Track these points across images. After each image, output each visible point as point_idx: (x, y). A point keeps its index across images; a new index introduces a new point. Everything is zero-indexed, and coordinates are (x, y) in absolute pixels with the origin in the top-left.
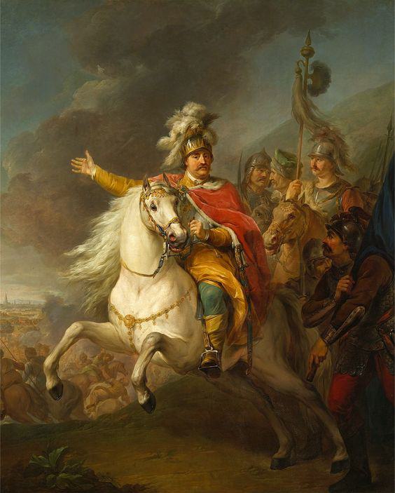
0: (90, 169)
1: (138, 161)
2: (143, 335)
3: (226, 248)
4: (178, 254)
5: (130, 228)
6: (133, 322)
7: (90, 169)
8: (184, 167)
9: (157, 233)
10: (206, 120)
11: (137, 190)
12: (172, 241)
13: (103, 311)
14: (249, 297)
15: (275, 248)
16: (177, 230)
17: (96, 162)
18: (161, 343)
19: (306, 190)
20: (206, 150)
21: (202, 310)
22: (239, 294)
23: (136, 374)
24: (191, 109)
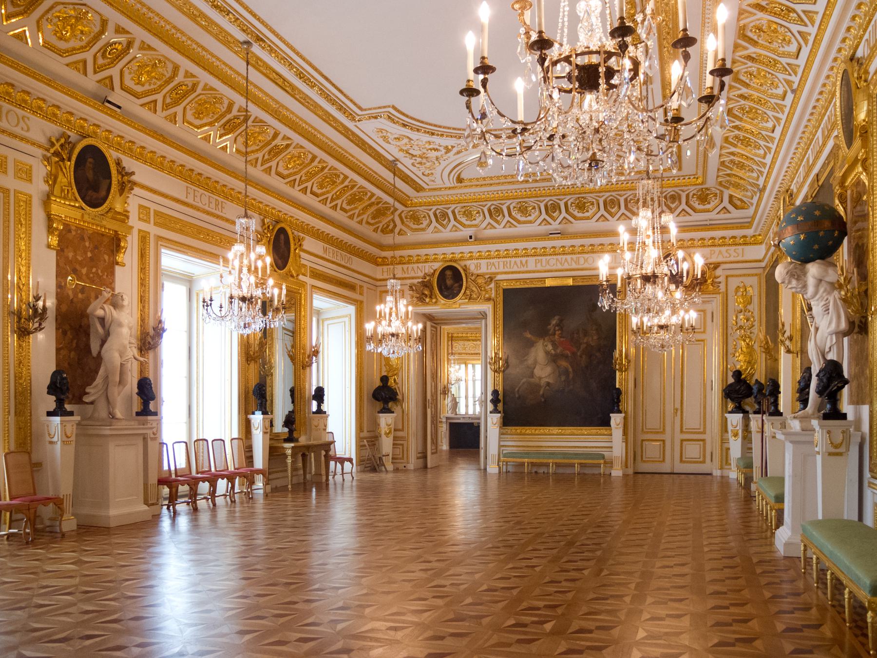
1: (543, 333)
2: (543, 382)
3: (567, 357)
4: (553, 359)
5: (540, 352)
6: (540, 378)
8: (555, 334)
9: (547, 353)
10: (561, 321)
11: (541, 342)
12: (551, 355)
14: (573, 370)
15: (581, 357)
16: (553, 352)
18: (548, 384)
19: (590, 339)
20: (561, 329)
21: (560, 376)
22: (571, 370)
23: (541, 393)
24: (557, 318)
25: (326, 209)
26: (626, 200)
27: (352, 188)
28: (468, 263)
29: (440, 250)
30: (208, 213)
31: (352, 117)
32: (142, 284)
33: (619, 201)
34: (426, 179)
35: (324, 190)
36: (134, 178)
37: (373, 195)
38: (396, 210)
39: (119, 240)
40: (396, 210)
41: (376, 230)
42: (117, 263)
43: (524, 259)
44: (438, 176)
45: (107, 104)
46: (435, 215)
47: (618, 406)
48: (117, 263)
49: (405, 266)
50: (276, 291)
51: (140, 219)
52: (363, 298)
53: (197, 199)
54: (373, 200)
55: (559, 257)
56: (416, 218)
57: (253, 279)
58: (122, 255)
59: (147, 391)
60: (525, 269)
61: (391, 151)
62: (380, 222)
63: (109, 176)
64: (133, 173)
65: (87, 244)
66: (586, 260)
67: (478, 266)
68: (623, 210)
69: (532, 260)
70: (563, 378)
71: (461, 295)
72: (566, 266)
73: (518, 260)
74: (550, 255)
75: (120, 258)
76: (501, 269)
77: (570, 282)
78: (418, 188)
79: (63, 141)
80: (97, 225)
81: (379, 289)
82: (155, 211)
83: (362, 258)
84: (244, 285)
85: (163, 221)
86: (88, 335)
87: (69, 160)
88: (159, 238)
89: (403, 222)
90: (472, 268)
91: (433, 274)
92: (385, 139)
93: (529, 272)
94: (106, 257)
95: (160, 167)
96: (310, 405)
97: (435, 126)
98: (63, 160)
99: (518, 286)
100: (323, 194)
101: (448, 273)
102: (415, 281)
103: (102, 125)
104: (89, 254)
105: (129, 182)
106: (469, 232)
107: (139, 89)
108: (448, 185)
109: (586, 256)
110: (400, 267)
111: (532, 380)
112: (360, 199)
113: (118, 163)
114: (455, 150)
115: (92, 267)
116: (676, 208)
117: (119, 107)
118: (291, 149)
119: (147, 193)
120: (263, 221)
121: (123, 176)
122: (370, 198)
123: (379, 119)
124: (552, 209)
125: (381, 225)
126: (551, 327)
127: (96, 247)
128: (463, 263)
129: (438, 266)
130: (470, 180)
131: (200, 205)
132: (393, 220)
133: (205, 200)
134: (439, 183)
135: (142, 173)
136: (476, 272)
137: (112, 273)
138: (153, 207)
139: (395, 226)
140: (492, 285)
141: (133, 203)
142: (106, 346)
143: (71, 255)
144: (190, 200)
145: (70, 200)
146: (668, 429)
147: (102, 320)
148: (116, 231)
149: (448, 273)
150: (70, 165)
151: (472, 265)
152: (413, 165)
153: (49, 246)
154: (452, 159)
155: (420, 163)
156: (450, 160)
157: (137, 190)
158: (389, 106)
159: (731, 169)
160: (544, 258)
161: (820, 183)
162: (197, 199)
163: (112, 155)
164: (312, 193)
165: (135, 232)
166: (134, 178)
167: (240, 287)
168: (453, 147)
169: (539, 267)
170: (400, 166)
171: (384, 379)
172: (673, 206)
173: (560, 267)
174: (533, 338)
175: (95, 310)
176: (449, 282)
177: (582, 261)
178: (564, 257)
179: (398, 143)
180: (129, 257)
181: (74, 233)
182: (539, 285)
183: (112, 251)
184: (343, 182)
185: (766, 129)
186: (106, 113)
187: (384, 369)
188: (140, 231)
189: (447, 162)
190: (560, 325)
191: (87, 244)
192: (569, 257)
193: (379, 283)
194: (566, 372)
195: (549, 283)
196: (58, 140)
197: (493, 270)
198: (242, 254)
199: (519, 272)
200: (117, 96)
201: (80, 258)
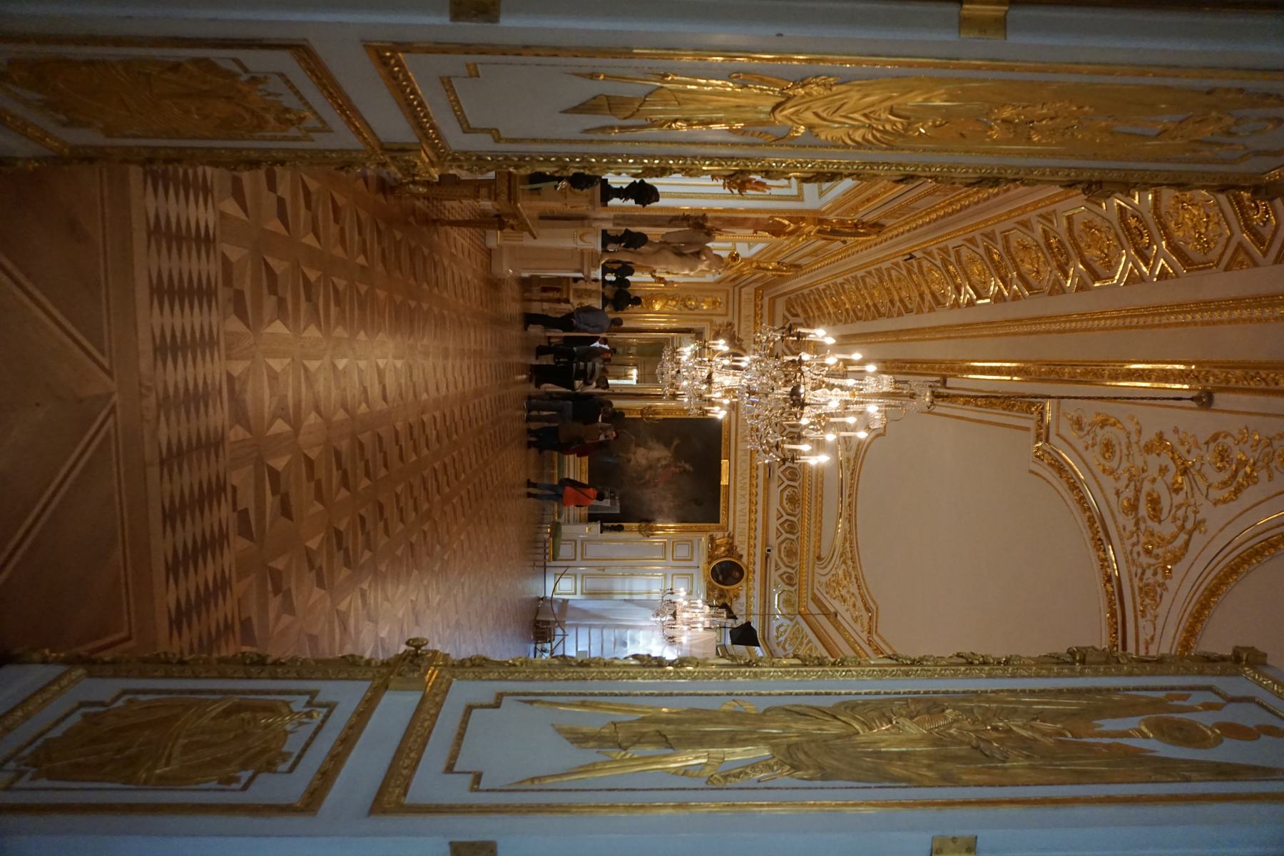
0: (676, 442)
2: (632, 456)
7: (676, 442)
9: (659, 460)
13: (638, 445)
18: (629, 461)
33: (793, 534)
66: (743, 496)
68: (785, 535)
72: (739, 478)
77: (724, 482)
102: (736, 329)
109: (747, 497)
110: (752, 313)
146: (585, 563)
171: (637, 301)
195: (724, 462)
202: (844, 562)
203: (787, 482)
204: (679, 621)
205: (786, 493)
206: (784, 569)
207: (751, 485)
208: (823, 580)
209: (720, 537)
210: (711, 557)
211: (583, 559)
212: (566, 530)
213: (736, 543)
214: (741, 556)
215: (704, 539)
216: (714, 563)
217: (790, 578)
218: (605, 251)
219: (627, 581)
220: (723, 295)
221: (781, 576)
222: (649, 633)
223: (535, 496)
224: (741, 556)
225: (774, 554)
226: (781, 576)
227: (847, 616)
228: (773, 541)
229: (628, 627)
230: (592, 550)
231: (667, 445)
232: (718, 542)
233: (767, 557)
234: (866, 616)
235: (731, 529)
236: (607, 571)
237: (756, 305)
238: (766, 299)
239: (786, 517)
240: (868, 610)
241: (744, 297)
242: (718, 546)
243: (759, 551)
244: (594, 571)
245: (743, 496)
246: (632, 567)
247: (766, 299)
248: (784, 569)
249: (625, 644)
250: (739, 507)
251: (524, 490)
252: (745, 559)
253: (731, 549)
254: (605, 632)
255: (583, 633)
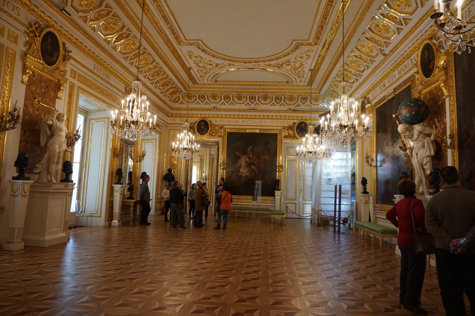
0: (238, 154)
1: (245, 153)
2: (244, 175)
5: (243, 161)
6: (243, 173)
7: (238, 154)
8: (250, 154)
9: (246, 162)
13: (239, 172)
17: (239, 153)
18: (246, 176)
20: (253, 152)
22: (256, 170)
23: (243, 180)
24: (251, 146)
25: (152, 87)
26: (284, 97)
27: (166, 79)
28: (211, 119)
29: (199, 112)
30: (103, 79)
31: (179, 42)
32: (69, 111)
33: (281, 98)
34: (200, 78)
35: (154, 78)
36: (70, 54)
37: (174, 83)
38: (181, 92)
39: (60, 86)
40: (181, 92)
41: (170, 100)
42: (58, 98)
43: (237, 120)
44: (206, 78)
45: (64, 12)
46: (199, 96)
47: (278, 187)
48: (58, 98)
49: (182, 118)
50: (151, 120)
51: (71, 76)
52: (162, 131)
53: (99, 71)
54: (173, 86)
55: (253, 120)
56: (189, 97)
57: (139, 111)
58: (60, 93)
59: (67, 168)
60: (237, 124)
61: (190, 63)
62: (173, 97)
63: (58, 50)
64: (70, 52)
65: (43, 84)
66: (265, 122)
67: (216, 121)
68: (282, 102)
69: (241, 120)
70: (253, 174)
71: (208, 133)
72: (256, 124)
73: (234, 120)
74: (245, 118)
75: (60, 94)
76: (227, 123)
77: (258, 131)
78: (195, 82)
79: (37, 25)
80: (50, 75)
81: (169, 128)
82: (79, 73)
83: (163, 113)
84: (134, 116)
85: (83, 80)
86: (39, 135)
87: (39, 36)
88: (80, 88)
89: (183, 98)
90: (213, 122)
91: (195, 123)
92: (190, 56)
93: (240, 125)
94: (52, 93)
95: (84, 51)
96: (139, 181)
97: (217, 53)
98: (36, 36)
99: (234, 131)
100: (152, 80)
101: (202, 123)
103: (58, 22)
104: (43, 90)
105: (68, 55)
106: (213, 105)
107: (80, 8)
108: (209, 82)
109: (265, 120)
110: (179, 118)
111: (239, 174)
112: (168, 85)
113: (64, 44)
114: (220, 66)
115: (44, 98)
116: (305, 103)
117: (70, 15)
118: (145, 55)
119: (76, 64)
120: (126, 88)
121: (66, 52)
122: (172, 85)
123: (193, 46)
124: (252, 98)
125: (173, 98)
126: (248, 150)
127: (47, 87)
128: (209, 119)
129: (198, 119)
130: (220, 81)
131: (100, 75)
132: (179, 97)
133: (102, 73)
134: (205, 82)
135: (75, 53)
136: (215, 124)
137: (54, 103)
138: (78, 71)
139: (179, 99)
140: (222, 130)
141: (69, 67)
142: (51, 141)
143: (33, 89)
144: (95, 71)
145: (37, 59)
146: (297, 198)
147: (50, 127)
148: (58, 80)
149: (202, 123)
150: (39, 40)
151: (213, 121)
152: (198, 71)
153: (22, 82)
154: (217, 70)
155: (201, 71)
156: (216, 70)
157: (71, 61)
158: (199, 40)
159: (333, 88)
160: (246, 120)
161: (396, 93)
162: (99, 71)
163: (61, 40)
164: (148, 78)
165: (68, 82)
166: (70, 54)
167: (132, 116)
168: (220, 64)
169: (244, 124)
170: (191, 71)
171: (170, 170)
172: (303, 102)
173: (253, 124)
174: (240, 155)
175: (48, 121)
176: (202, 127)
177: (263, 122)
178: (255, 120)
179: (195, 59)
180: (63, 94)
181: (36, 77)
182: (244, 131)
183: (55, 91)
184: (163, 75)
185: (359, 71)
186: (62, 16)
187: (169, 165)
188: (70, 82)
189: (214, 71)
190: (252, 149)
191: (43, 84)
192: (257, 120)
193: (168, 125)
194: (254, 171)
195: (248, 131)
196: (34, 25)
197: (223, 123)
198: (134, 99)
199: (235, 125)
200: (69, 8)
201: (38, 92)
202: (282, 65)
203: (257, 101)
204: (313, 150)
205: (262, 101)
206: (299, 102)
207: (259, 119)
208: (298, 80)
209: (285, 133)
210: (294, 137)
211: (295, 200)
212: (277, 208)
213: (287, 125)
214: (294, 123)
215: (285, 141)
216: (297, 136)
217: (304, 99)
218: (122, 184)
219: (307, 178)
220: (171, 131)
221: (303, 104)
222: (323, 166)
223: (225, 225)
224: (294, 123)
225: (292, 107)
226: (303, 104)
227: (309, 61)
228: (286, 108)
229: (320, 177)
230: (291, 195)
231: (239, 158)
232: (287, 134)
233: (294, 111)
234: (302, 49)
235: (280, 128)
236: (302, 188)
237: (176, 117)
238: (173, 112)
239: (274, 101)
240: (297, 47)
241: (172, 122)
242: (289, 134)
243: (291, 115)
244: (302, 194)
245: (265, 122)
246: (300, 177)
247: (173, 112)
248: (299, 102)
249: (330, 179)
250: (270, 124)
251: (221, 230)
252: (296, 121)
253: (290, 128)
254: (323, 189)
255: (323, 201)
